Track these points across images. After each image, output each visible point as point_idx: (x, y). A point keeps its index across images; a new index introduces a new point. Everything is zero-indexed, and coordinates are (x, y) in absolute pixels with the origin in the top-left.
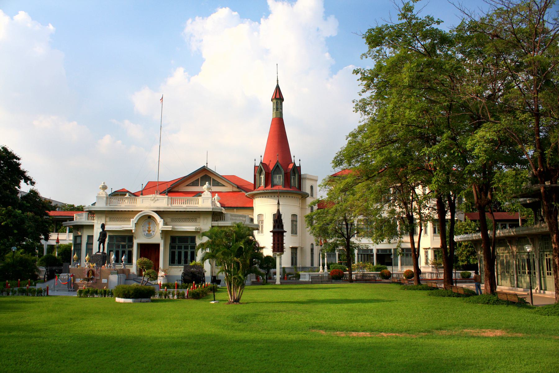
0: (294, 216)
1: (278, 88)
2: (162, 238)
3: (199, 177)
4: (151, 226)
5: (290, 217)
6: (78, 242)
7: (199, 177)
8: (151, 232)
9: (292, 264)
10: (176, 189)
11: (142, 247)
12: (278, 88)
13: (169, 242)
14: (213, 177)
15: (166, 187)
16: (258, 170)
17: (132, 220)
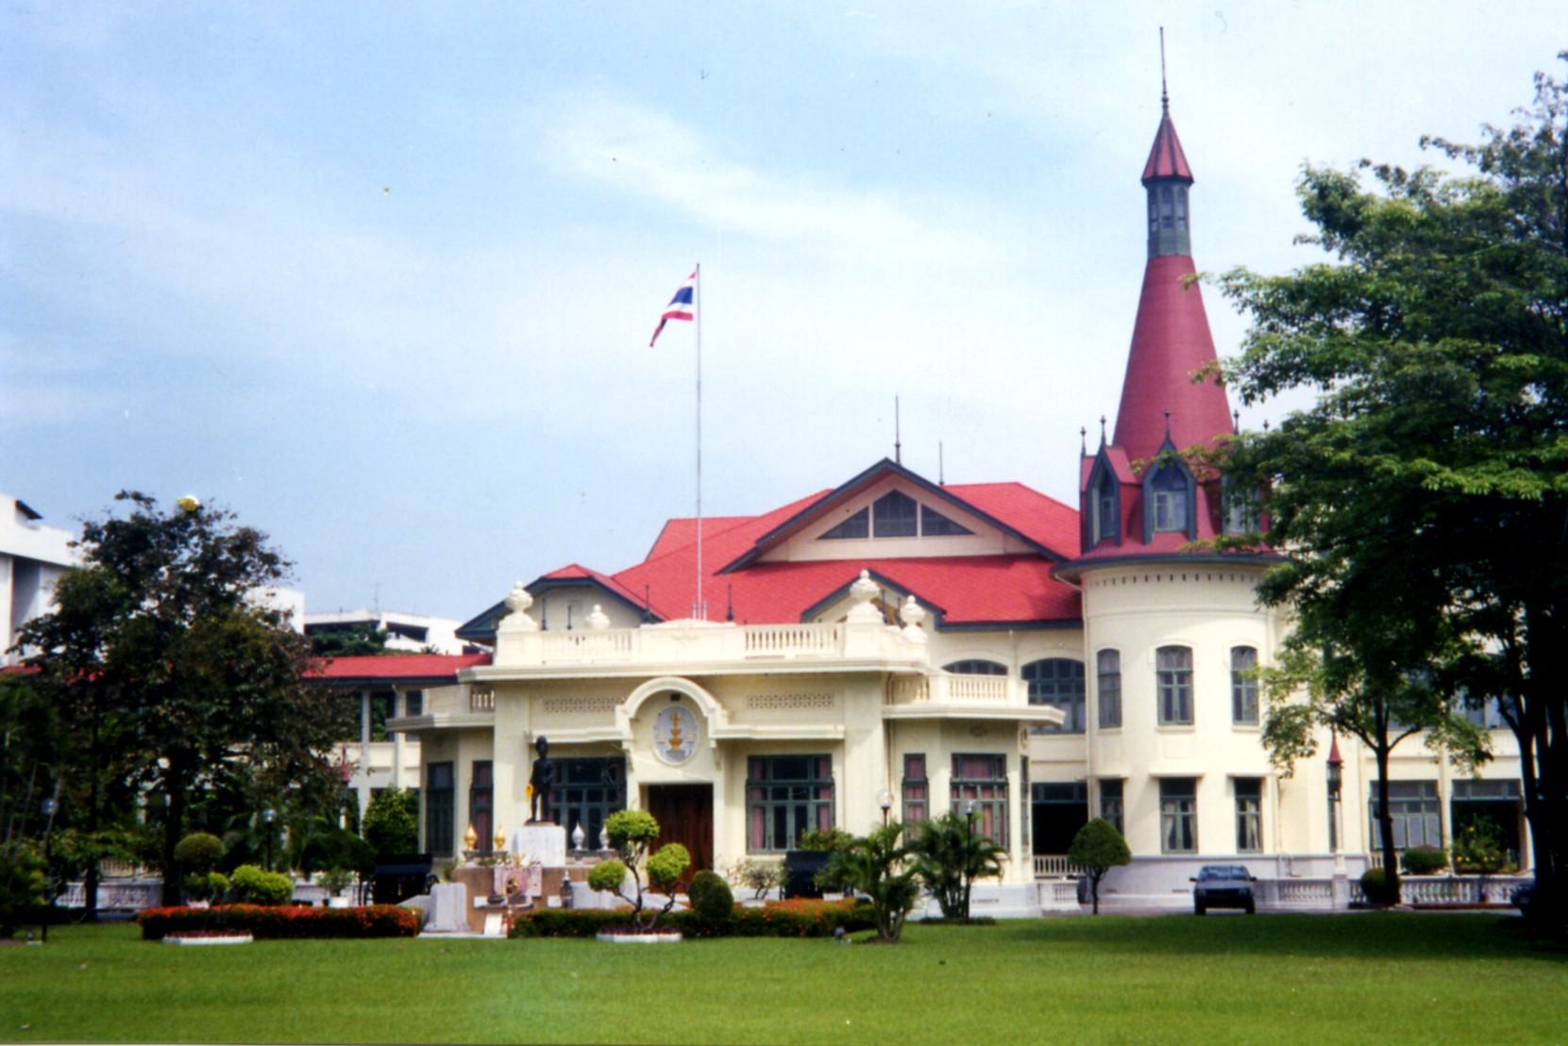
0: (1243, 653)
1: (1166, 135)
2: (718, 764)
3: (867, 501)
4: (680, 726)
5: (1228, 657)
6: (441, 782)
7: (867, 501)
8: (682, 747)
9: (1243, 841)
10: (778, 555)
11: (658, 796)
12: (1166, 135)
13: (742, 777)
14: (922, 499)
15: (746, 544)
16: (1098, 474)
17: (618, 708)
